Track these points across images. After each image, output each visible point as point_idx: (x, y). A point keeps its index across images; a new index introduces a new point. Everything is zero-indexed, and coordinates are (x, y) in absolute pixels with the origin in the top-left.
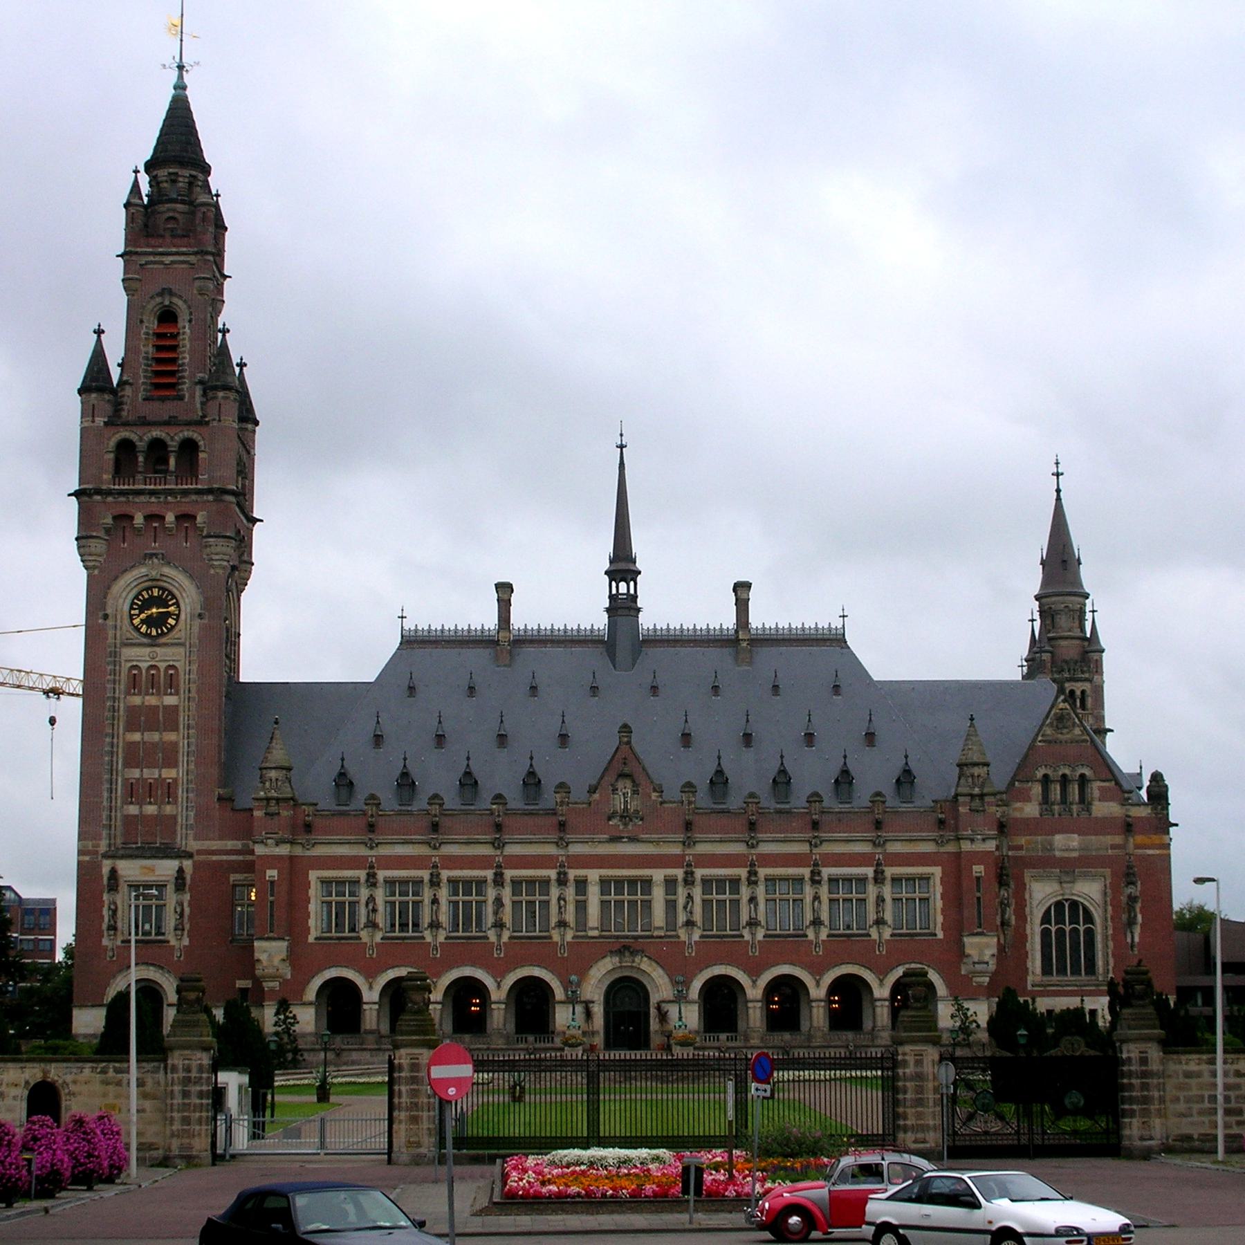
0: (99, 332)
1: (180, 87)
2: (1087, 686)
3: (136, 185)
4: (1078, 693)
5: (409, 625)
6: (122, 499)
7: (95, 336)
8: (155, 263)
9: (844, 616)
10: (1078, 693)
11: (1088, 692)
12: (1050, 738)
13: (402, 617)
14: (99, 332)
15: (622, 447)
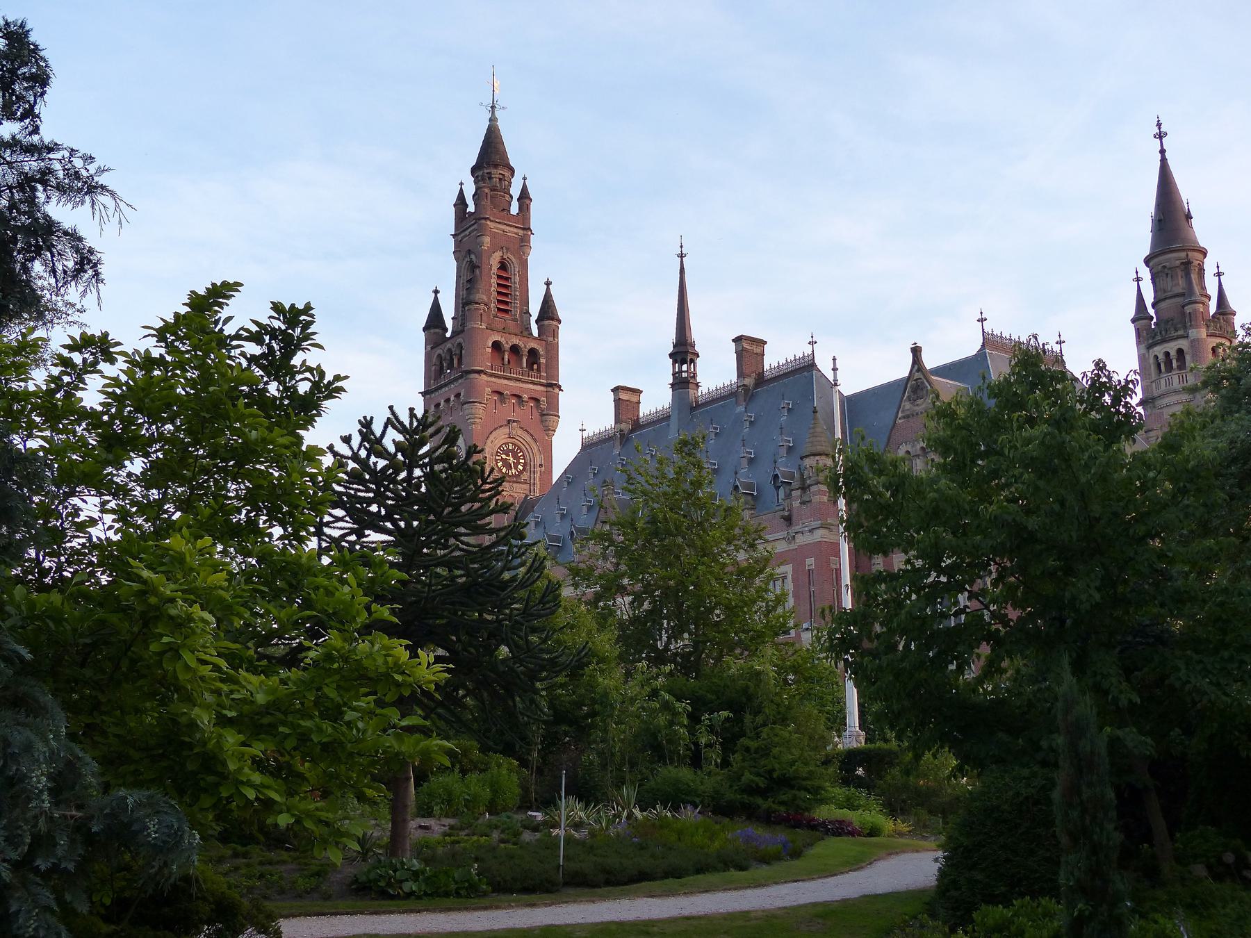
0: (436, 292)
1: (493, 120)
2: (1183, 344)
3: (461, 192)
4: (1173, 353)
5: (585, 435)
6: (437, 394)
7: (434, 295)
8: (465, 236)
9: (812, 343)
10: (1173, 353)
11: (1185, 349)
12: (908, 413)
13: (582, 430)
14: (436, 292)
15: (682, 256)
